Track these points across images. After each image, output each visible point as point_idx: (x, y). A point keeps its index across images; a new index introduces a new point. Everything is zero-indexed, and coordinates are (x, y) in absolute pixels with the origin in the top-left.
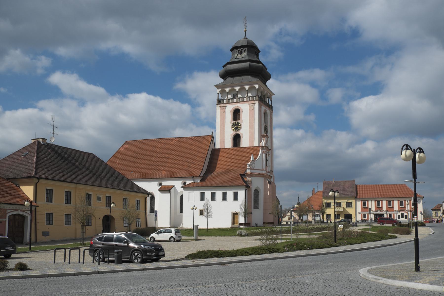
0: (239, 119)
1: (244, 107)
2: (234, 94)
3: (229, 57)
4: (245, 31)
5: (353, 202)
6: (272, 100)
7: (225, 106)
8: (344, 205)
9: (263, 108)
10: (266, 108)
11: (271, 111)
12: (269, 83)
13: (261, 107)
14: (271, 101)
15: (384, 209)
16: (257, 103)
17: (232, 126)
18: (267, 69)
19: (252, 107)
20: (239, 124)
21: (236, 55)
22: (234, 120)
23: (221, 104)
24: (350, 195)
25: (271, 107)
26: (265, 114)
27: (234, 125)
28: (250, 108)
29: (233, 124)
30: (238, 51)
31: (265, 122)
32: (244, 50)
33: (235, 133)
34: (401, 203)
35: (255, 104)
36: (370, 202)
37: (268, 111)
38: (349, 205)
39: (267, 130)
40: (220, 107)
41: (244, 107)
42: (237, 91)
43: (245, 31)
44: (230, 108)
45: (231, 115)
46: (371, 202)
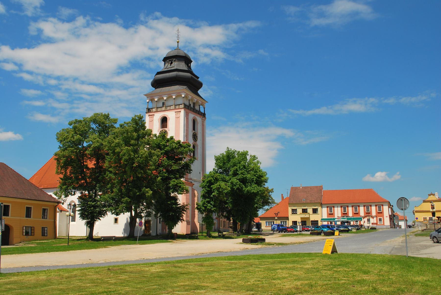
0: (166, 127)
1: (171, 115)
2: (163, 103)
3: (162, 66)
4: (178, 42)
5: (319, 209)
6: (205, 107)
7: (153, 114)
8: (310, 210)
9: (192, 116)
10: (194, 116)
11: (204, 118)
12: (200, 92)
13: (188, 115)
14: (204, 108)
15: (350, 214)
16: (183, 111)
18: (198, 78)
19: (178, 115)
20: (166, 131)
21: (167, 65)
22: (162, 128)
23: (150, 113)
24: (316, 201)
25: (203, 115)
26: (194, 121)
28: (176, 116)
29: (161, 132)
30: (168, 62)
31: (194, 129)
32: (174, 60)
34: (330, 210)
35: (180, 112)
36: (336, 209)
37: (199, 119)
38: (315, 211)
39: (197, 137)
40: (149, 115)
41: (171, 115)
42: (165, 100)
43: (178, 42)
44: (158, 116)
45: (159, 123)
46: (337, 208)
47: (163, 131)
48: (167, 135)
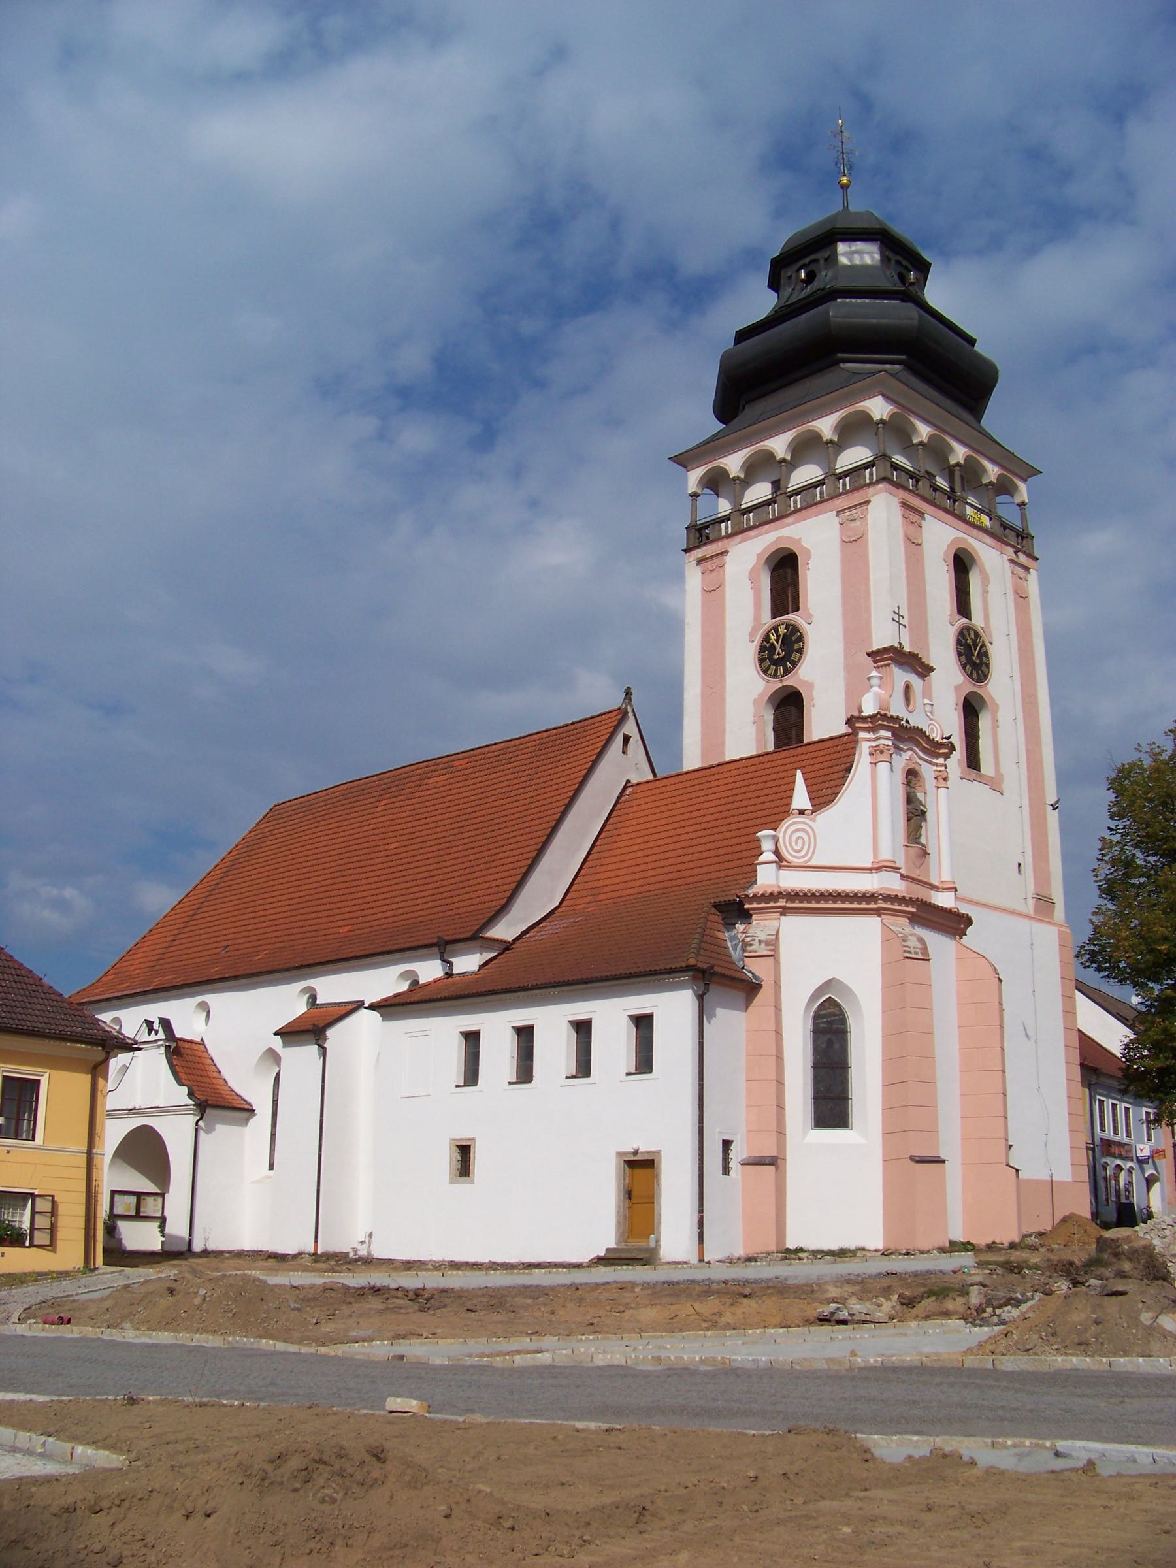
33: (970, 687)
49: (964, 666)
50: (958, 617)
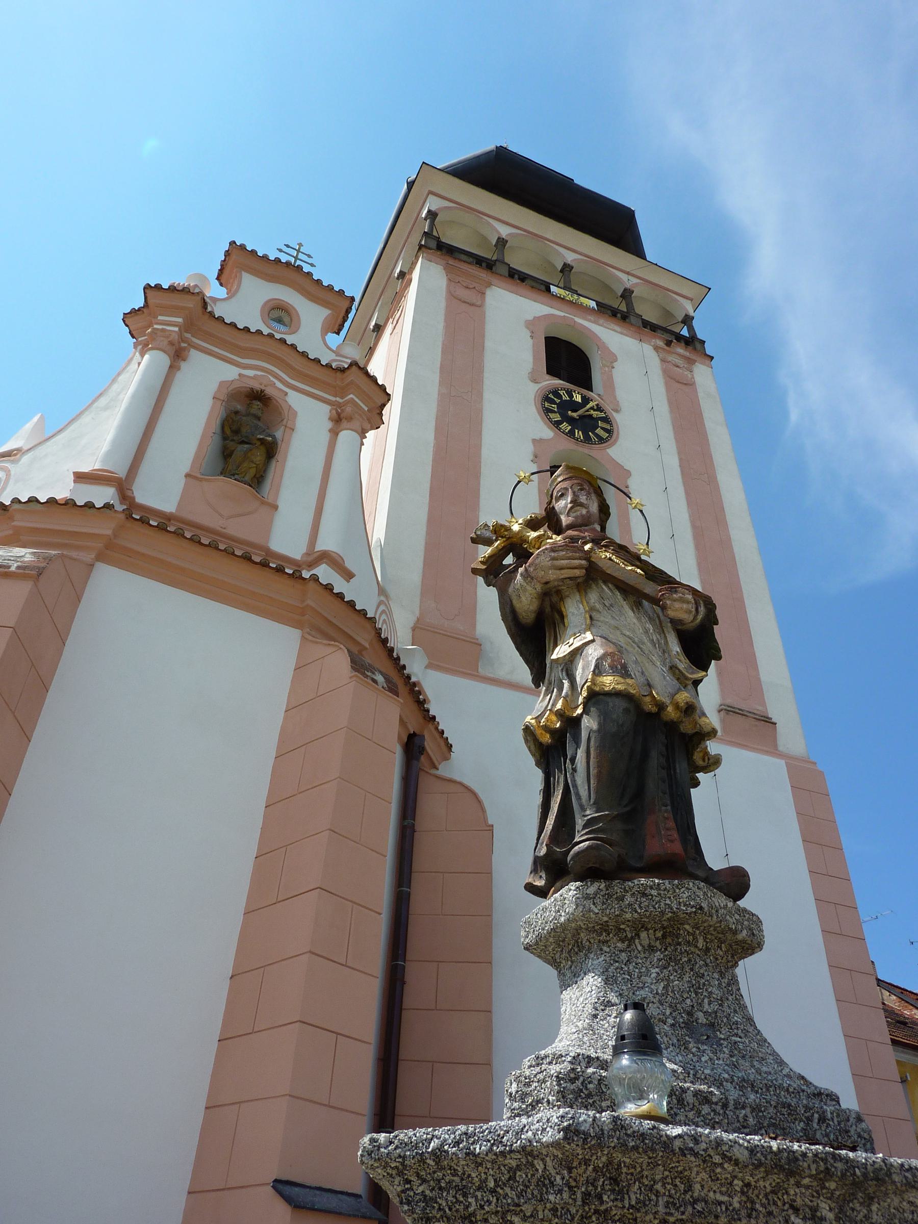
17: (546, 399)
27: (558, 401)
29: (556, 393)
47: (570, 393)
48: (609, 432)
49: (557, 424)
50: (548, 377)
